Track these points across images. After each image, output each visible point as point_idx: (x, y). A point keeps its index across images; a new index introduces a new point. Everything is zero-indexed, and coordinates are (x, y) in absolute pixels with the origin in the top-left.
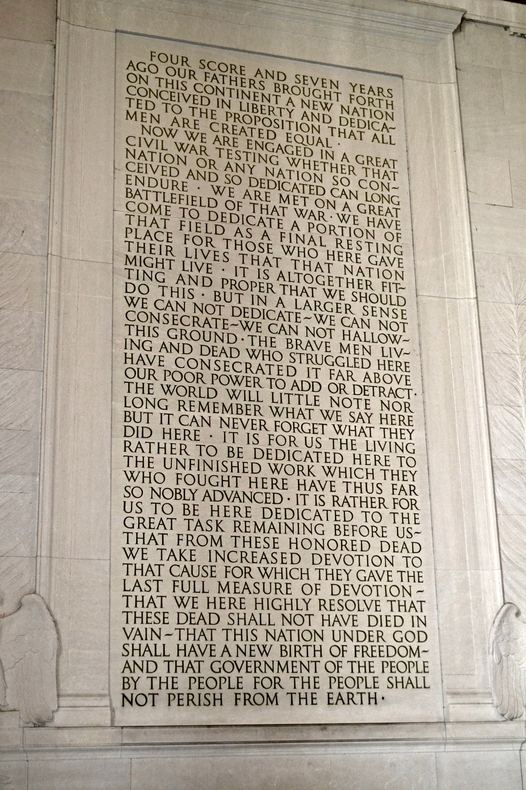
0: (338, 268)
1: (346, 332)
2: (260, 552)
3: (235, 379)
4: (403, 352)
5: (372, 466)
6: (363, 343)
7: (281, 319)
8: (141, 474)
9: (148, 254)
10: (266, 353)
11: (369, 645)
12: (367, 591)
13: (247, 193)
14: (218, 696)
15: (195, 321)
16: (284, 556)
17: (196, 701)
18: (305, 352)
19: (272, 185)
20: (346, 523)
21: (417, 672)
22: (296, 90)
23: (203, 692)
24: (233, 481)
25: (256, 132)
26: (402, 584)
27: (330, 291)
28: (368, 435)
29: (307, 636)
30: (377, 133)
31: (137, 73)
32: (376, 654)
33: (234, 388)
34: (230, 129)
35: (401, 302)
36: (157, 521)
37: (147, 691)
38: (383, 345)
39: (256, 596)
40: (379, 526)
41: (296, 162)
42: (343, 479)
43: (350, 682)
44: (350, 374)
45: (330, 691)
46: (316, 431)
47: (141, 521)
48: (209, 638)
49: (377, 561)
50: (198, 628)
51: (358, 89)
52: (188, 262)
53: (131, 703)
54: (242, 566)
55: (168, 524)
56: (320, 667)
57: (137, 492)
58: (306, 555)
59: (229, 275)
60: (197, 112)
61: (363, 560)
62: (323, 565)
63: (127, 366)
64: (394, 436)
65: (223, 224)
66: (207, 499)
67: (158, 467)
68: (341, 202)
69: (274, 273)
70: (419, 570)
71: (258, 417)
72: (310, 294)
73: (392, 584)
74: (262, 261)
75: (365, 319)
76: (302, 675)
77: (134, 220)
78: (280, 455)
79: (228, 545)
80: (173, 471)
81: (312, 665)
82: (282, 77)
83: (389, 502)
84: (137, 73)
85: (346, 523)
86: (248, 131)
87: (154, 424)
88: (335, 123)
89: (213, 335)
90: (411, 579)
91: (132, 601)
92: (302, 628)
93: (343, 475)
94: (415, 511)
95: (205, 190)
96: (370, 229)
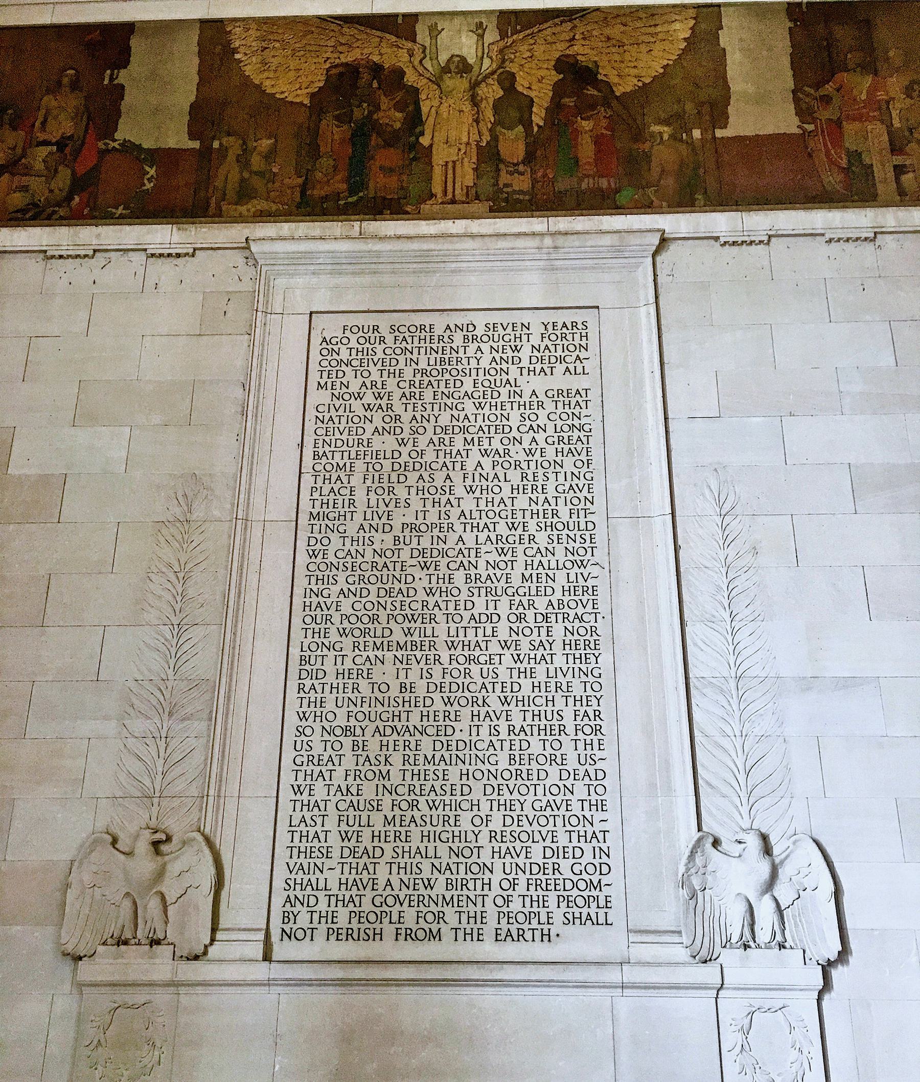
0: (522, 502)
1: (529, 562)
2: (429, 785)
3: (410, 617)
4: (591, 575)
5: (553, 693)
6: (547, 571)
7: (461, 556)
8: (313, 713)
9: (331, 509)
10: (444, 589)
11: (543, 878)
12: (543, 821)
13: (431, 441)
14: (378, 931)
15: (374, 565)
16: (454, 787)
17: (355, 936)
18: (484, 585)
19: (457, 430)
20: (521, 752)
21: (598, 907)
22: (485, 339)
23: (363, 927)
24: (404, 716)
25: (443, 384)
26: (583, 813)
27: (513, 524)
28: (549, 662)
29: (475, 869)
30: (569, 365)
31: (330, 347)
32: (552, 887)
33: (409, 626)
34: (417, 385)
35: (590, 526)
36: (326, 758)
37: (306, 925)
38: (568, 571)
39: (422, 829)
40: (558, 754)
41: (482, 405)
42: (520, 707)
43: (521, 918)
44: (531, 602)
45: (499, 926)
46: (492, 662)
47: (311, 758)
48: (372, 871)
49: (555, 790)
50: (362, 862)
51: (550, 327)
52: (369, 511)
53: (290, 938)
54: (409, 799)
55: (336, 762)
56: (489, 901)
57: (308, 731)
58: (477, 787)
59: (410, 519)
60: (385, 373)
61: (540, 790)
62: (495, 796)
63: (305, 613)
64: (578, 661)
65: (406, 473)
66: (377, 734)
67: (330, 705)
68: (527, 439)
69: (455, 512)
70: (602, 798)
71: (433, 652)
72: (492, 529)
73: (572, 813)
74: (443, 502)
75: (550, 547)
76: (468, 909)
77: (320, 480)
78: (454, 687)
79: (396, 778)
80: (345, 709)
81: (480, 899)
82: (471, 328)
83: (570, 729)
84: (330, 347)
85: (521, 752)
86: (435, 384)
87: (329, 666)
88: (525, 363)
89: (391, 578)
90: (594, 808)
91: (297, 836)
92: (470, 861)
93: (520, 704)
94: (600, 736)
95: (390, 443)
96: (558, 460)
